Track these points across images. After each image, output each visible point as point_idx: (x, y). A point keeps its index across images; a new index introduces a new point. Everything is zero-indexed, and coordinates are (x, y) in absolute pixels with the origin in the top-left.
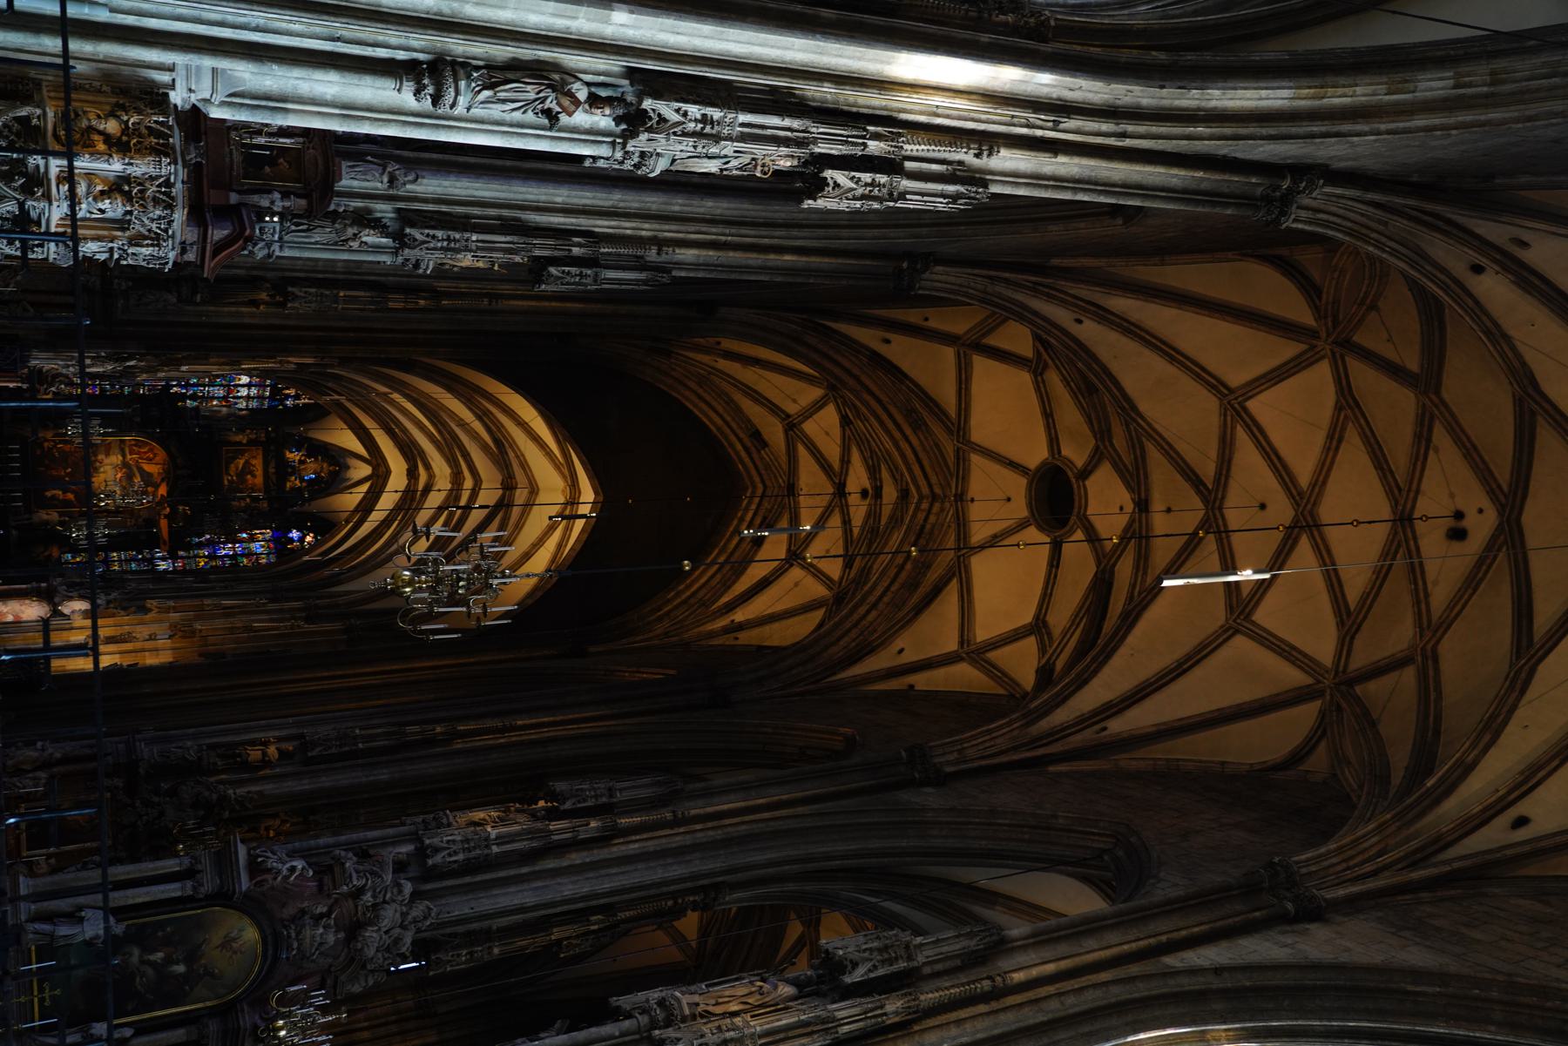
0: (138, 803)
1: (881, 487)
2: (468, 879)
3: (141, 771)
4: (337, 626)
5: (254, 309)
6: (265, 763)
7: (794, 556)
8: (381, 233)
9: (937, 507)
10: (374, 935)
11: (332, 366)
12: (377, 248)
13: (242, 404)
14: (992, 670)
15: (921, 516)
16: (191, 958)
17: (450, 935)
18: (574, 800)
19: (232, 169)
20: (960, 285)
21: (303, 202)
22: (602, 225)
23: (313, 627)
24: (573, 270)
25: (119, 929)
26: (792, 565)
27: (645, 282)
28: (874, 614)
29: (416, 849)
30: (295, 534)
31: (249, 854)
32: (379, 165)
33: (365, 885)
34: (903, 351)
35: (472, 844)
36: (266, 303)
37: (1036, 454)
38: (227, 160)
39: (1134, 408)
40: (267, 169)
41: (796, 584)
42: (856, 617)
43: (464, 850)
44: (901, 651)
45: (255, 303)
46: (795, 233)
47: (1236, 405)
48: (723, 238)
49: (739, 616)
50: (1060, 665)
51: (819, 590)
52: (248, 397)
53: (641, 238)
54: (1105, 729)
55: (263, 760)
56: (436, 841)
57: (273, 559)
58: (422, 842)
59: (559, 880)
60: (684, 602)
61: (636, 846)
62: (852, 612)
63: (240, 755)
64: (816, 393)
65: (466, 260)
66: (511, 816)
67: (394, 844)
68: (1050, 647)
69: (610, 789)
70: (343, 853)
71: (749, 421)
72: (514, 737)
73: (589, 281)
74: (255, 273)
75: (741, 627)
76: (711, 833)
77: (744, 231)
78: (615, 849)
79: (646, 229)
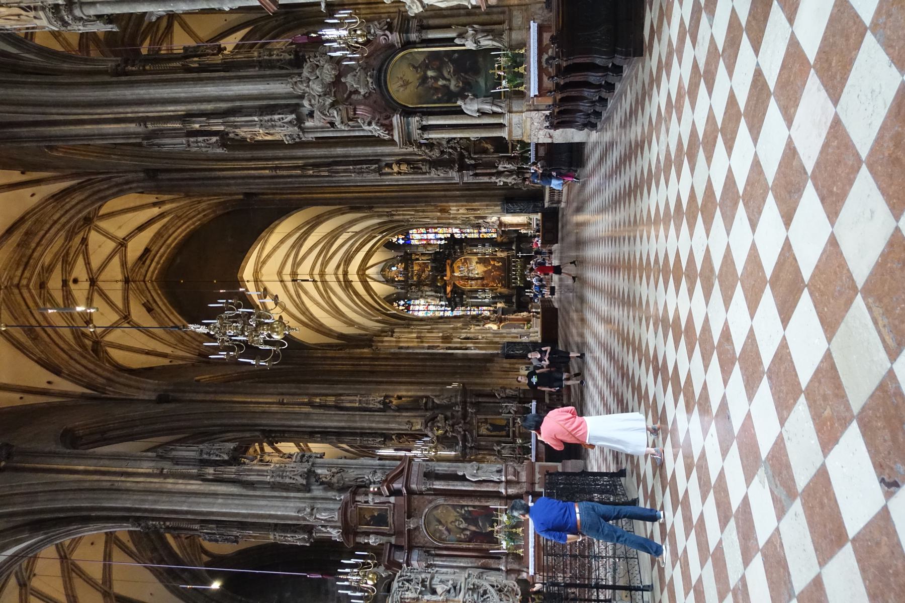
0: (459, 149)
1: (63, 286)
2: (272, 102)
3: (456, 165)
5: (400, 394)
6: (399, 163)
7: (122, 244)
8: (320, 478)
9: (16, 281)
11: (378, 331)
12: (322, 466)
13: (422, 301)
15: (27, 274)
16: (424, 79)
18: (211, 142)
19: (393, 514)
21: (358, 499)
22: (195, 486)
23: (387, 210)
25: (459, 103)
26: (124, 239)
28: (55, 217)
29: (304, 123)
30: (401, 242)
31: (392, 135)
33: (330, 108)
34: (40, 377)
35: (270, 124)
36: (393, 397)
38: (395, 517)
41: (120, 227)
42: (68, 216)
43: (274, 121)
44: (33, 195)
45: (399, 398)
46: (75, 486)
48: (123, 479)
49: (156, 211)
51: (104, 224)
52: (418, 305)
53: (174, 478)
55: (400, 164)
56: (291, 129)
57: (411, 232)
58: (300, 127)
60: (190, 219)
63: (411, 168)
64: (109, 338)
66: (249, 136)
67: (317, 128)
69: (189, 145)
70: (343, 128)
71: (154, 318)
72: (270, 164)
73: (205, 451)
74: (397, 414)
75: (154, 204)
76: (121, 110)
79: (170, 484)
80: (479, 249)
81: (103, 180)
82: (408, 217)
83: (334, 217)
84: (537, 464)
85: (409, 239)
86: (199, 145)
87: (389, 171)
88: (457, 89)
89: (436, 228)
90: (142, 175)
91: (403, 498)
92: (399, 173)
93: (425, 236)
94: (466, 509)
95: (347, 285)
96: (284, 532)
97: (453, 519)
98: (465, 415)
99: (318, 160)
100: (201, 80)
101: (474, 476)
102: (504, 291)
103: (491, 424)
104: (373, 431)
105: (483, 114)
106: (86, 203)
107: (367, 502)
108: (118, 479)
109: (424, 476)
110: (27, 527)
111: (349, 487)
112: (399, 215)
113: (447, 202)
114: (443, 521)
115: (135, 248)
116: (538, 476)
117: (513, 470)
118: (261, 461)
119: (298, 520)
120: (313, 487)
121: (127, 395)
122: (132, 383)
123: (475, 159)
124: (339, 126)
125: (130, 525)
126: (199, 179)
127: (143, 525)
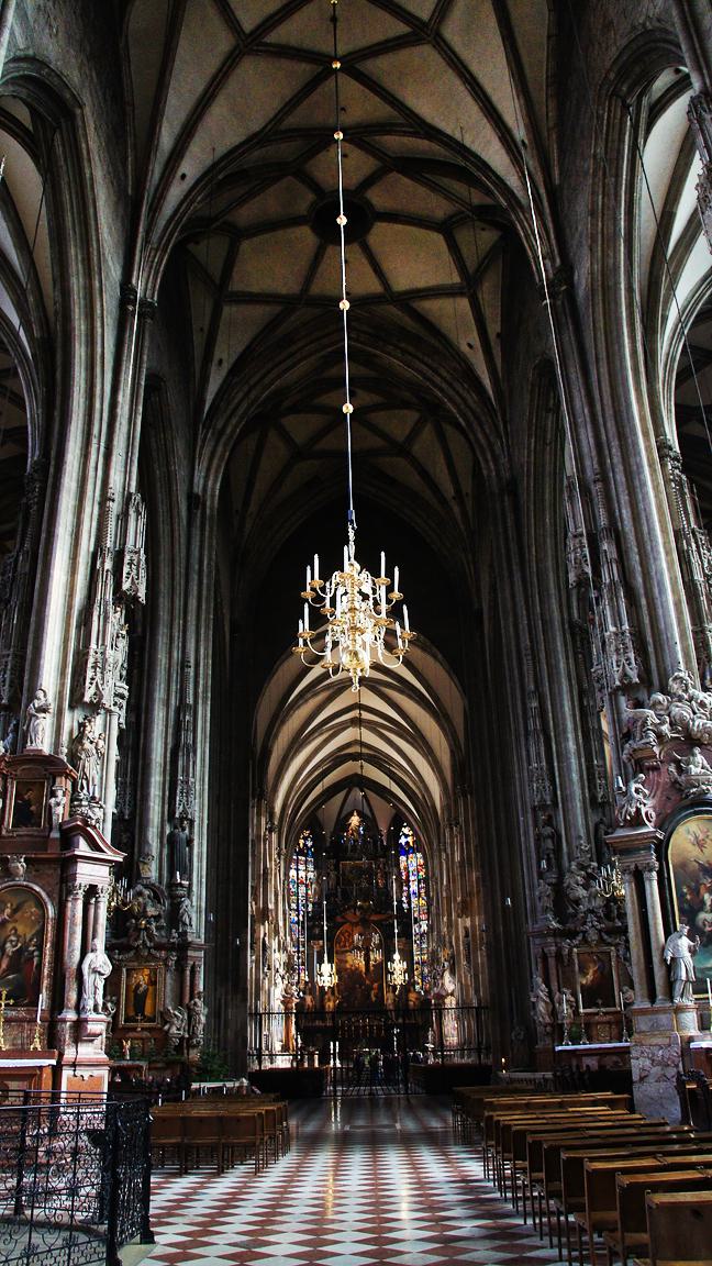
2: (651, 649)
4: (461, 803)
5: (196, 843)
8: (90, 721)
10: (696, 724)
11: (273, 808)
12: (106, 726)
13: (311, 875)
14: (483, 268)
17: (698, 664)
20: (151, 268)
21: (58, 780)
22: (87, 545)
23: (461, 819)
24: (126, 569)
27: (138, 513)
30: (403, 841)
32: (30, 720)
33: (654, 732)
34: (227, 352)
37: (305, 236)
38: (25, 839)
39: (255, 135)
40: (33, 808)
42: (444, 385)
44: (470, 346)
45: (190, 842)
47: (249, 40)
48: (102, 449)
50: (477, 198)
51: (428, 433)
52: (306, 870)
53: (99, 515)
54: (523, 141)
56: (617, 676)
57: (419, 855)
59: (653, 573)
61: (624, 511)
62: (442, 390)
64: (273, 436)
65: (117, 655)
67: (619, 713)
68: (463, 212)
69: (575, 536)
70: (625, 752)
75: (458, 491)
77: (95, 431)
78: (627, 529)
80: (398, 966)
81: (496, 427)
82: (449, 851)
83: (448, 740)
84: (104, 1073)
85: (406, 853)
86: (577, 550)
87: (540, 823)
88: (700, 924)
89: (427, 894)
90: (506, 475)
91: (59, 852)
92: (539, 838)
93: (412, 878)
94: (36, 953)
95: (337, 759)
96: (12, 669)
97: (21, 929)
98: (159, 947)
99: (550, 715)
100: (668, 553)
101: (89, 968)
102: (330, 1005)
103: (146, 991)
104: (138, 803)
105: (671, 967)
106: (463, 407)
107: (53, 794)
108: (102, 444)
109: (90, 885)
110: (46, 335)
111: (75, 766)
112: (452, 837)
113: (486, 913)
114: (18, 915)
115: (399, 467)
116: (85, 1073)
117: (98, 1032)
118: (118, 637)
119: (28, 690)
120: (76, 711)
121: (200, 454)
122: (215, 461)
123: (571, 951)
124: (627, 745)
125: (35, 458)
126: (508, 550)
127: (36, 476)
